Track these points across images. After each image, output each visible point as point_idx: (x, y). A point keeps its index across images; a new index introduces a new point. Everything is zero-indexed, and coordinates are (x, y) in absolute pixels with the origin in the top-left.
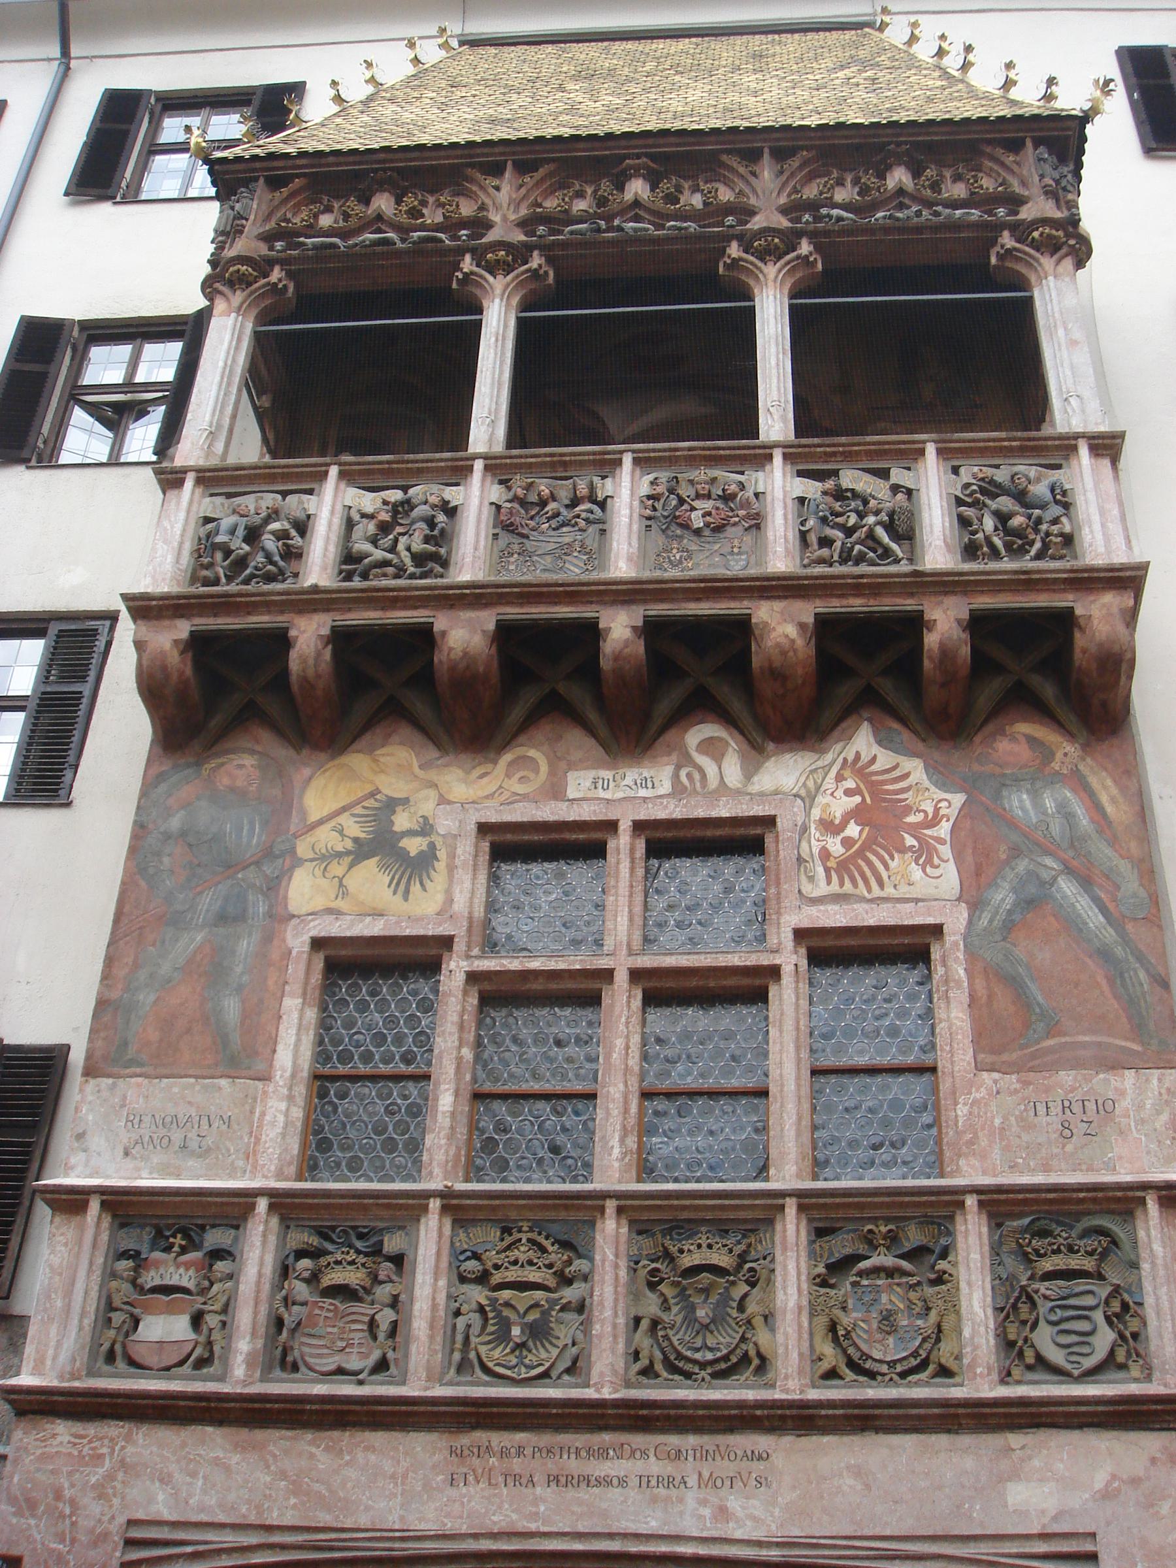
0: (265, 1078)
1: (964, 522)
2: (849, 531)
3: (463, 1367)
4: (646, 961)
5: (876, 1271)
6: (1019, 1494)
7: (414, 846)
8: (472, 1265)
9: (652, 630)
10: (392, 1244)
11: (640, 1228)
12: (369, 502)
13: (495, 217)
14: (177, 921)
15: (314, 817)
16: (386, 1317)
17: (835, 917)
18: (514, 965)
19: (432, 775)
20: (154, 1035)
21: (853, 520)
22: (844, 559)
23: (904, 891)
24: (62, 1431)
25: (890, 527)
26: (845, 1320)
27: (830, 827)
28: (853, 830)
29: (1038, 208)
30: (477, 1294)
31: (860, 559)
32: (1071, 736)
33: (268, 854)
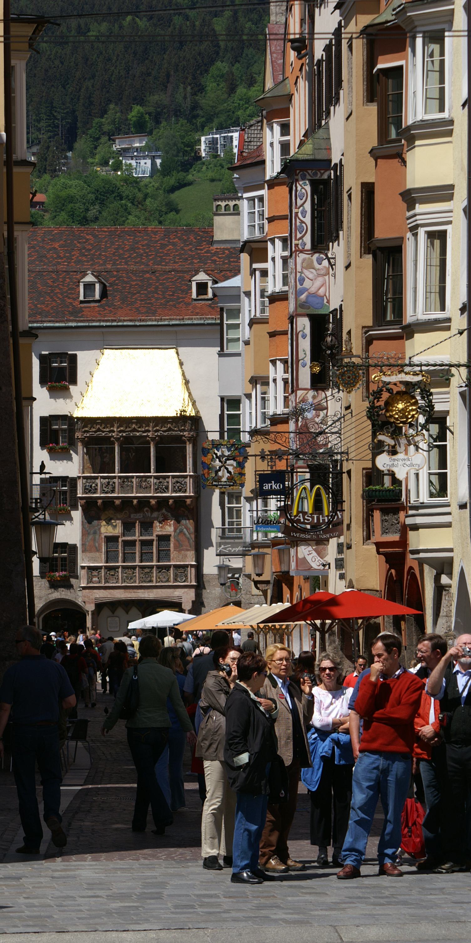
1: (174, 487)
4: (141, 538)
6: (175, 593)
13: (115, 430)
14: (89, 534)
17: (160, 533)
30: (125, 575)
31: (162, 493)
33: (98, 525)
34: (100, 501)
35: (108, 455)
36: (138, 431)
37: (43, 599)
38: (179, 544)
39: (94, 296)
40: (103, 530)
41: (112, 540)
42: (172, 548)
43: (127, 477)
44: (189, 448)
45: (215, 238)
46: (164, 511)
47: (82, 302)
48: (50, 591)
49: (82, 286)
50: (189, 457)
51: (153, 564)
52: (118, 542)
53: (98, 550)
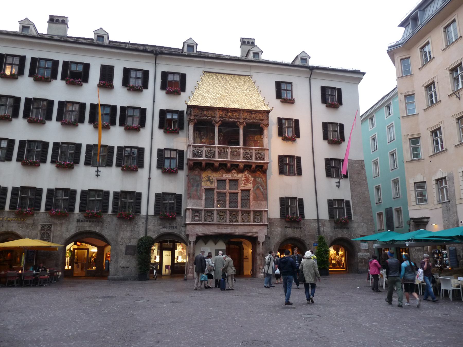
0: (202, 200)
1: (256, 156)
2: (247, 156)
3: (218, 221)
4: (230, 191)
5: (245, 215)
6: (254, 230)
7: (212, 180)
8: (218, 214)
9: (231, 165)
10: (212, 212)
11: (229, 212)
12: (207, 149)
14: (193, 186)
15: (203, 177)
16: (212, 218)
17: (243, 188)
18: (220, 191)
19: (213, 174)
20: (193, 196)
21: (247, 155)
22: (247, 159)
23: (249, 186)
24: (190, 226)
25: (250, 157)
26: (243, 218)
27: (243, 181)
28: (245, 181)
29: (265, 122)
30: (219, 216)
31: (248, 160)
32: (262, 173)
33: (200, 180)
34: (204, 163)
35: (205, 138)
36: (232, 118)
37: (156, 232)
38: (257, 196)
40: (203, 184)
43: (223, 148)
44: (265, 132)
46: (246, 173)
50: (266, 137)
51: (239, 209)
53: (200, 198)
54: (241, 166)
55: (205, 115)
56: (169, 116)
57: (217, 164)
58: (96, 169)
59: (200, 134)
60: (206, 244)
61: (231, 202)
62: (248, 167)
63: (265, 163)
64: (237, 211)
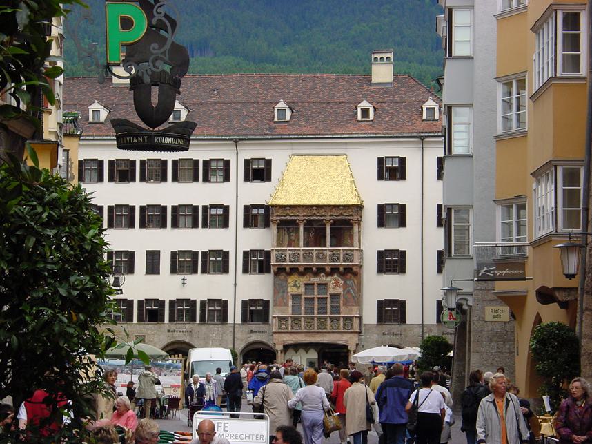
12: (291, 253)
17: (332, 293)
29: (355, 218)
34: (288, 268)
36: (317, 216)
39: (285, 119)
40: (289, 290)
41: (296, 297)
42: (341, 305)
43: (308, 250)
44: (356, 228)
45: (373, 82)
46: (336, 276)
47: (275, 122)
48: (249, 336)
49: (276, 109)
52: (301, 299)
54: (328, 269)
55: (288, 214)
56: (255, 212)
57: (301, 269)
58: (181, 277)
59: (288, 229)
60: (296, 352)
61: (319, 308)
62: (334, 270)
63: (353, 265)
64: (326, 318)
